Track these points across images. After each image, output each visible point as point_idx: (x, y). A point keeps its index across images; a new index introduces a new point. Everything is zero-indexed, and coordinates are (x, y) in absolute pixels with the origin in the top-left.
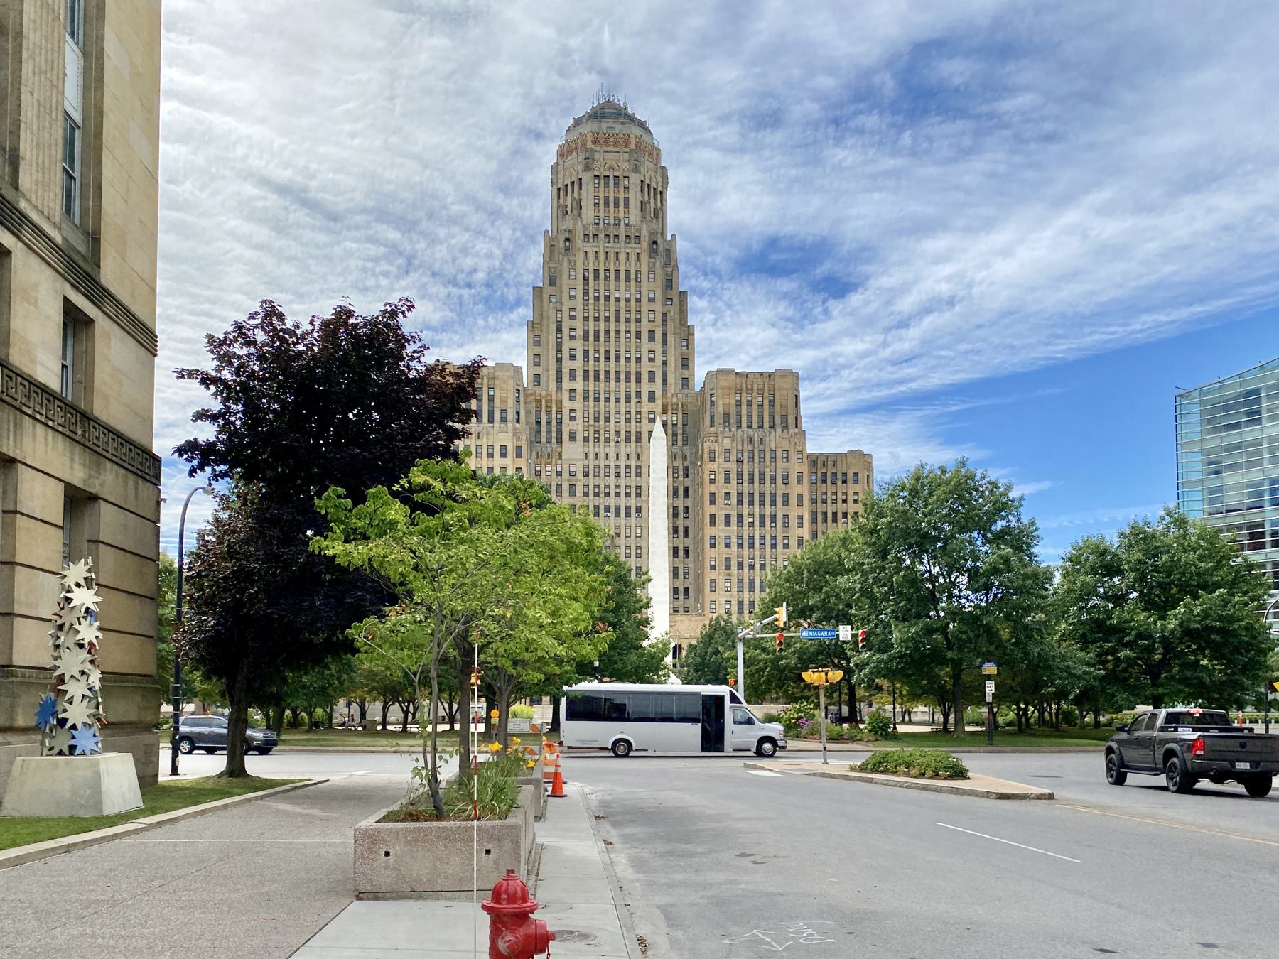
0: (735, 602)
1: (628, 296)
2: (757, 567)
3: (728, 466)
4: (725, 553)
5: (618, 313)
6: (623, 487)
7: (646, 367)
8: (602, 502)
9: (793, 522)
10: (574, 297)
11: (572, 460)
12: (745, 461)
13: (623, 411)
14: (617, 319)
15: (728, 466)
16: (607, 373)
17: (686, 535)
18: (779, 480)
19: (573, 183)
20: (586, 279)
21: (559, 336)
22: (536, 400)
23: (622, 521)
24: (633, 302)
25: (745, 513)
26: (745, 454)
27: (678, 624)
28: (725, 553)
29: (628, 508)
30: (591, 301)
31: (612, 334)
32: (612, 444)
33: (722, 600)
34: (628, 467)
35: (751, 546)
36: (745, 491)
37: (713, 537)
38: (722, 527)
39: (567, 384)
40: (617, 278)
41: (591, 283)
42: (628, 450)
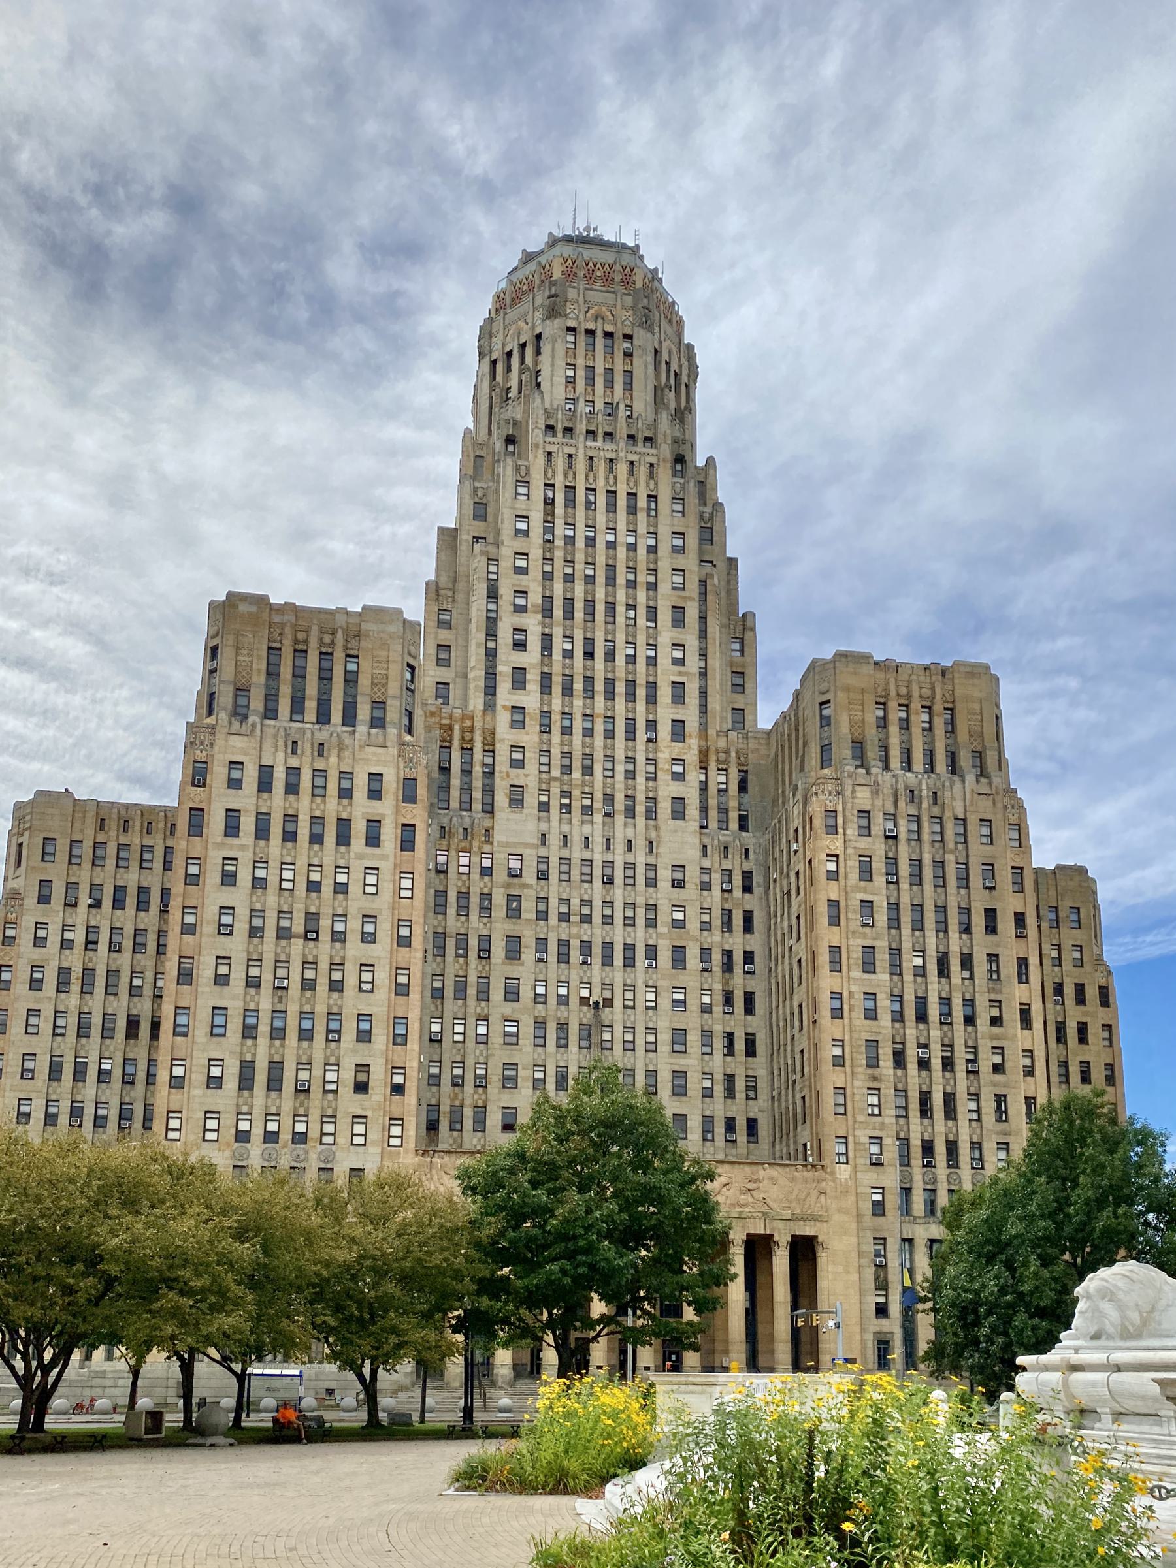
0: (890, 1142)
1: (631, 540)
2: (936, 1063)
3: (864, 844)
4: (864, 1029)
5: (611, 568)
6: (619, 905)
8: (577, 933)
9: (1009, 969)
10: (526, 533)
11: (515, 845)
13: (620, 755)
14: (611, 581)
15: (864, 844)
16: (589, 680)
18: (976, 880)
19: (523, 346)
20: (549, 503)
21: (492, 607)
22: (441, 727)
23: (618, 975)
24: (642, 552)
25: (907, 946)
27: (764, 1184)
28: (864, 1029)
29: (630, 948)
30: (559, 542)
31: (600, 608)
32: (598, 818)
33: (863, 1136)
34: (630, 866)
35: (922, 1017)
36: (905, 900)
37: (837, 996)
38: (857, 973)
39: (505, 695)
40: (612, 507)
41: (559, 509)
42: (630, 833)
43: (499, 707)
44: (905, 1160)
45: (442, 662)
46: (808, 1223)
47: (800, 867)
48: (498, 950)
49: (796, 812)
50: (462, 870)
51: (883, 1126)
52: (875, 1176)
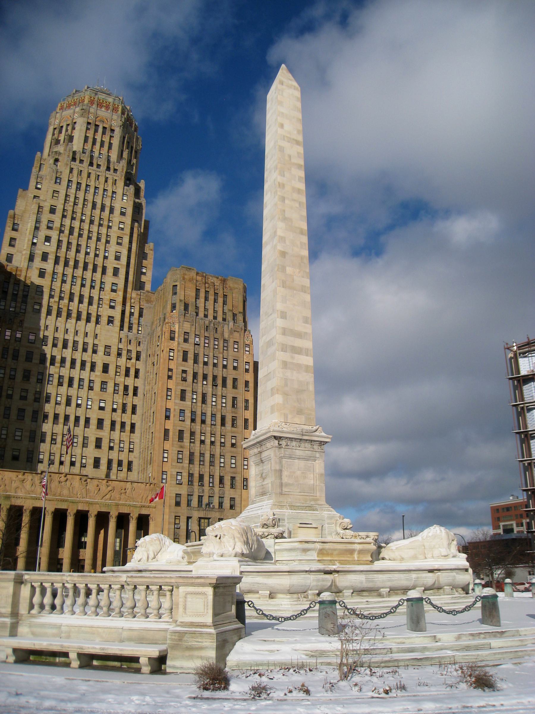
0: (185, 474)
3: (186, 346)
7: (111, 264)
12: (202, 344)
15: (186, 346)
17: (134, 412)
26: (203, 339)
34: (85, 344)
38: (178, 401)
39: (38, 263)
43: (34, 268)
44: (190, 482)
45: (11, 245)
46: (147, 509)
47: (159, 353)
48: (19, 376)
49: (159, 329)
50: (7, 338)
51: (183, 468)
52: (178, 489)
